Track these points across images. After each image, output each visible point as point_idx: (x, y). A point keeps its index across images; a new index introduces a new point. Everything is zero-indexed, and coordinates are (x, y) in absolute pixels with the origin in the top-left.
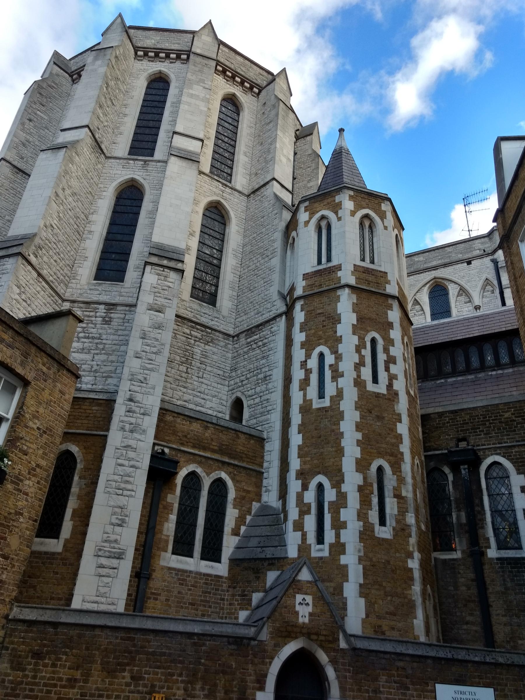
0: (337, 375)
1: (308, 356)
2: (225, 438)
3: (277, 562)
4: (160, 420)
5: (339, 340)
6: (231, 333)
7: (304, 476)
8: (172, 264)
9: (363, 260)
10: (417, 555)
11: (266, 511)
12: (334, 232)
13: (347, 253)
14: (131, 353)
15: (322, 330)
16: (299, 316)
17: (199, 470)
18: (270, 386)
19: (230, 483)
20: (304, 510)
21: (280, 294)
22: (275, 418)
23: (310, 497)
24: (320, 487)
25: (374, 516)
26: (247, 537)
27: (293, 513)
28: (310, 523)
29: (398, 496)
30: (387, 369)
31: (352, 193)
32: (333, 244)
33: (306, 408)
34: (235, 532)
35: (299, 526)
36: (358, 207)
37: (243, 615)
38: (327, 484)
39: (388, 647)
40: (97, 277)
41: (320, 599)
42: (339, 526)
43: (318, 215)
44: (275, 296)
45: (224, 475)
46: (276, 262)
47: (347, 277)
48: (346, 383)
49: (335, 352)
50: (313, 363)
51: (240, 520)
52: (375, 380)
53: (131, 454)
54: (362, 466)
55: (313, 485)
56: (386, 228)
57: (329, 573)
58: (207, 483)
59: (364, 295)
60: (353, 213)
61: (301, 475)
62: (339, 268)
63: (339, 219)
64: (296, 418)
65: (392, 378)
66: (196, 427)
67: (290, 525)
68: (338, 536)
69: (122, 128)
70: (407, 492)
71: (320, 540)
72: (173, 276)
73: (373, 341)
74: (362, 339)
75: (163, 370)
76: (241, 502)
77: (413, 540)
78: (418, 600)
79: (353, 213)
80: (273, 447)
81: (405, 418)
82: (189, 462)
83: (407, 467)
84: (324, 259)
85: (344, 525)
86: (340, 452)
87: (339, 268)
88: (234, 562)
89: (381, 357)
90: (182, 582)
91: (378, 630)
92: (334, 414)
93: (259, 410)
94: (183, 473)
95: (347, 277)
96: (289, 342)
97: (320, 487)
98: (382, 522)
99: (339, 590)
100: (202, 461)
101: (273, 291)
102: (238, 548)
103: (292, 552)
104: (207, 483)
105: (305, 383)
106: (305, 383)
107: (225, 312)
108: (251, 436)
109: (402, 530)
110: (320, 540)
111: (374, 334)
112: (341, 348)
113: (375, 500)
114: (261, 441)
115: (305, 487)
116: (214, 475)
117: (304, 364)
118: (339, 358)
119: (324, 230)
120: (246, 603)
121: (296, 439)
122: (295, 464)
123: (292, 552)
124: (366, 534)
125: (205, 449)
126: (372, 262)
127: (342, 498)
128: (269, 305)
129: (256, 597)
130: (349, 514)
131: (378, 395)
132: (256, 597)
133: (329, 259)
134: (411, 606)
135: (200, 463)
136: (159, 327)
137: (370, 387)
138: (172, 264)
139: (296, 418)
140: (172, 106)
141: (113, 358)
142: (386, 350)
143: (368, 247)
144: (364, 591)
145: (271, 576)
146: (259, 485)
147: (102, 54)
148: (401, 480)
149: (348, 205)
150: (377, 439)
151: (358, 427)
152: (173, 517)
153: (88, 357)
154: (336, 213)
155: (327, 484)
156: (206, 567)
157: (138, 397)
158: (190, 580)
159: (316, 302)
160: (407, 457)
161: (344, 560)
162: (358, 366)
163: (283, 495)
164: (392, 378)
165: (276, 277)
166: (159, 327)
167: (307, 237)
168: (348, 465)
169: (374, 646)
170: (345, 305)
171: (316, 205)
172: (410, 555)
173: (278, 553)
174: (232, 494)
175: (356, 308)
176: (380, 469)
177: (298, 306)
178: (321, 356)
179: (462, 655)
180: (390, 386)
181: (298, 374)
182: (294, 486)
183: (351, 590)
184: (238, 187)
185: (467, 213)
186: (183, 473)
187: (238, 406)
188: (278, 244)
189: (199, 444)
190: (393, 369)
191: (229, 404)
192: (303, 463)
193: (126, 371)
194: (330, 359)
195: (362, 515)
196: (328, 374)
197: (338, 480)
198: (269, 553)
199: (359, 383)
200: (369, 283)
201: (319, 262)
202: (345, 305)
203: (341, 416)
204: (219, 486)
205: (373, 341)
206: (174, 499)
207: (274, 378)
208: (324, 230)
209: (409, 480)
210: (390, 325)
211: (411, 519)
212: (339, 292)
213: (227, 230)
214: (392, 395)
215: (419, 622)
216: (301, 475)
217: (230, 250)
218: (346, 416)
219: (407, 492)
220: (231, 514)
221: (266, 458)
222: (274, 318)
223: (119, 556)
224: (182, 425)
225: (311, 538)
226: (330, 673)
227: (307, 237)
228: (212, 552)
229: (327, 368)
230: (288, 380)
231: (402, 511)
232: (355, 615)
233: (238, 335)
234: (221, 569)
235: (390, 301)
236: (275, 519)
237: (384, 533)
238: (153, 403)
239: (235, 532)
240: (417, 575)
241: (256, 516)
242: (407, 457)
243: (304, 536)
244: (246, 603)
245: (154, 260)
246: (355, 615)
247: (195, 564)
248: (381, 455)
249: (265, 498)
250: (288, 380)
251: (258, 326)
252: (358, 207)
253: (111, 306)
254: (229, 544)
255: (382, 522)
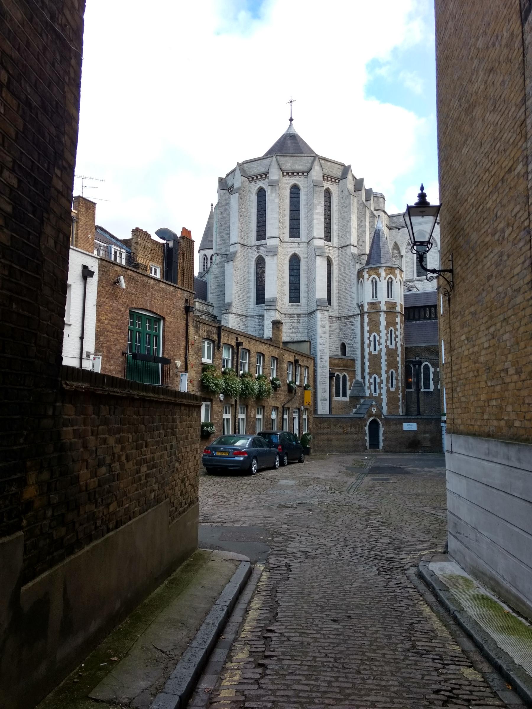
0: (380, 344)
1: (370, 336)
2: (344, 362)
3: (364, 397)
4: (329, 362)
5: (380, 331)
6: (338, 316)
7: (370, 374)
8: (325, 308)
9: (388, 297)
10: (401, 394)
11: (357, 382)
12: (378, 286)
13: (383, 298)
14: (318, 343)
15: (375, 327)
16: (366, 320)
17: (339, 374)
18: (356, 341)
19: (347, 375)
20: (371, 384)
21: (358, 304)
22: (359, 353)
23: (372, 380)
24: (375, 378)
25: (390, 385)
26: (353, 390)
27: (367, 385)
28: (372, 387)
29: (397, 379)
30: (395, 340)
31: (385, 268)
32: (378, 292)
33: (370, 354)
34: (350, 389)
35: (369, 388)
36: (387, 274)
37: (354, 410)
38: (377, 377)
39: (393, 417)
40: (290, 301)
41: (377, 408)
42: (380, 388)
43: (372, 277)
44: (356, 306)
45: (345, 373)
46: (354, 289)
47: (383, 307)
48: (383, 346)
49: (379, 336)
50: (372, 338)
51: (351, 385)
52: (391, 344)
53: (324, 374)
54: (387, 372)
55: (373, 377)
56: (397, 282)
57: (379, 400)
58: (341, 376)
59: (389, 313)
60: (385, 278)
61: (369, 374)
62: (380, 303)
63: (380, 281)
64: (367, 357)
65: (397, 342)
66: (337, 361)
67: (366, 388)
68: (380, 391)
69: (285, 224)
70: (399, 378)
71: (375, 391)
72: (326, 312)
73: (391, 330)
74: (388, 331)
75: (328, 347)
76: (351, 380)
77: (400, 390)
78: (401, 405)
79: (385, 278)
80: (358, 363)
81: (400, 355)
82: (336, 371)
83: (399, 371)
84: (374, 297)
85: (382, 388)
86: (381, 368)
87: (380, 303)
88: (350, 397)
89: (394, 336)
90: (339, 404)
91: (390, 413)
92: (378, 356)
93: (352, 349)
94: (335, 375)
95: (383, 307)
96: (362, 328)
97: (375, 378)
98: (392, 387)
99: (381, 404)
100: (340, 371)
101: (355, 303)
102: (351, 393)
103: (368, 395)
104: (341, 376)
105: (369, 345)
106: (369, 345)
107: (335, 308)
108: (351, 360)
109: (397, 388)
110: (375, 391)
111: (392, 328)
112: (381, 334)
113: (390, 381)
114: (354, 361)
115: (371, 378)
116: (343, 374)
117: (369, 338)
118: (380, 338)
119: (374, 283)
120: (355, 407)
121: (367, 363)
122: (367, 371)
123: (368, 395)
124: (388, 391)
125: (339, 367)
126: (391, 297)
127: (381, 381)
128: (353, 309)
129: (358, 406)
130: (383, 386)
131: (392, 349)
132: (358, 406)
133: (376, 297)
134: (399, 406)
135: (339, 371)
136: (325, 333)
137: (390, 347)
138: (325, 308)
139: (367, 357)
140: (304, 208)
141: (303, 335)
142: (395, 333)
143: (390, 293)
144: (387, 404)
145: (362, 401)
146: (355, 374)
147: (274, 189)
148: (398, 375)
149: (383, 274)
150: (392, 364)
151: (386, 361)
152: (334, 388)
153: (295, 335)
154: (379, 278)
155: (377, 377)
156: (344, 399)
157: (323, 357)
158: (340, 403)
159: (372, 316)
160: (400, 368)
161: (382, 397)
162: (386, 341)
163: (363, 377)
164: (397, 342)
165: (355, 296)
166: (325, 333)
167: (368, 286)
168: (383, 372)
169: (390, 417)
170: (382, 318)
171: (371, 271)
172: (399, 394)
173: (363, 395)
174: (348, 378)
175: (386, 320)
176: (392, 372)
177: (366, 316)
178: (375, 336)
179: (410, 417)
180: (396, 345)
181: (367, 342)
182: (367, 377)
183: (384, 404)
184: (335, 245)
185: (436, 224)
186: (335, 375)
187: (343, 347)
188: (355, 281)
189: (338, 366)
190: (397, 339)
191: (340, 344)
192: (370, 371)
193: (318, 350)
194: (377, 338)
195: (387, 386)
196: (377, 343)
197: (380, 376)
198: (361, 395)
199: (387, 346)
200: (390, 308)
201: (373, 298)
202: (382, 318)
203: (381, 357)
204: (344, 377)
205: (391, 330)
206: (334, 383)
207: (357, 338)
208: (374, 283)
209: (400, 374)
210: (397, 323)
211: (400, 385)
212: (381, 313)
213: (332, 268)
214: (397, 348)
215: (400, 410)
216: (369, 374)
217: (334, 279)
218: (383, 357)
219: (399, 378)
220: (348, 384)
221: (356, 366)
222: (356, 315)
223: (326, 400)
224: (333, 361)
225: (373, 391)
226: (380, 423)
227: (368, 286)
228: (344, 395)
229: (376, 341)
230: (363, 343)
231: (398, 383)
232: (385, 409)
233: (341, 317)
234: (347, 399)
235: (397, 314)
236: (361, 385)
237: (392, 389)
238: (327, 358)
239: (350, 389)
240: (401, 399)
241: (355, 383)
242: (400, 368)
243: (371, 391)
244: (355, 407)
245: (319, 308)
246: (385, 409)
247: (341, 399)
248: (392, 368)
249: (357, 378)
250: (363, 343)
251: (349, 316)
252: (387, 274)
253: (299, 315)
254: (348, 392)
255: (392, 387)
